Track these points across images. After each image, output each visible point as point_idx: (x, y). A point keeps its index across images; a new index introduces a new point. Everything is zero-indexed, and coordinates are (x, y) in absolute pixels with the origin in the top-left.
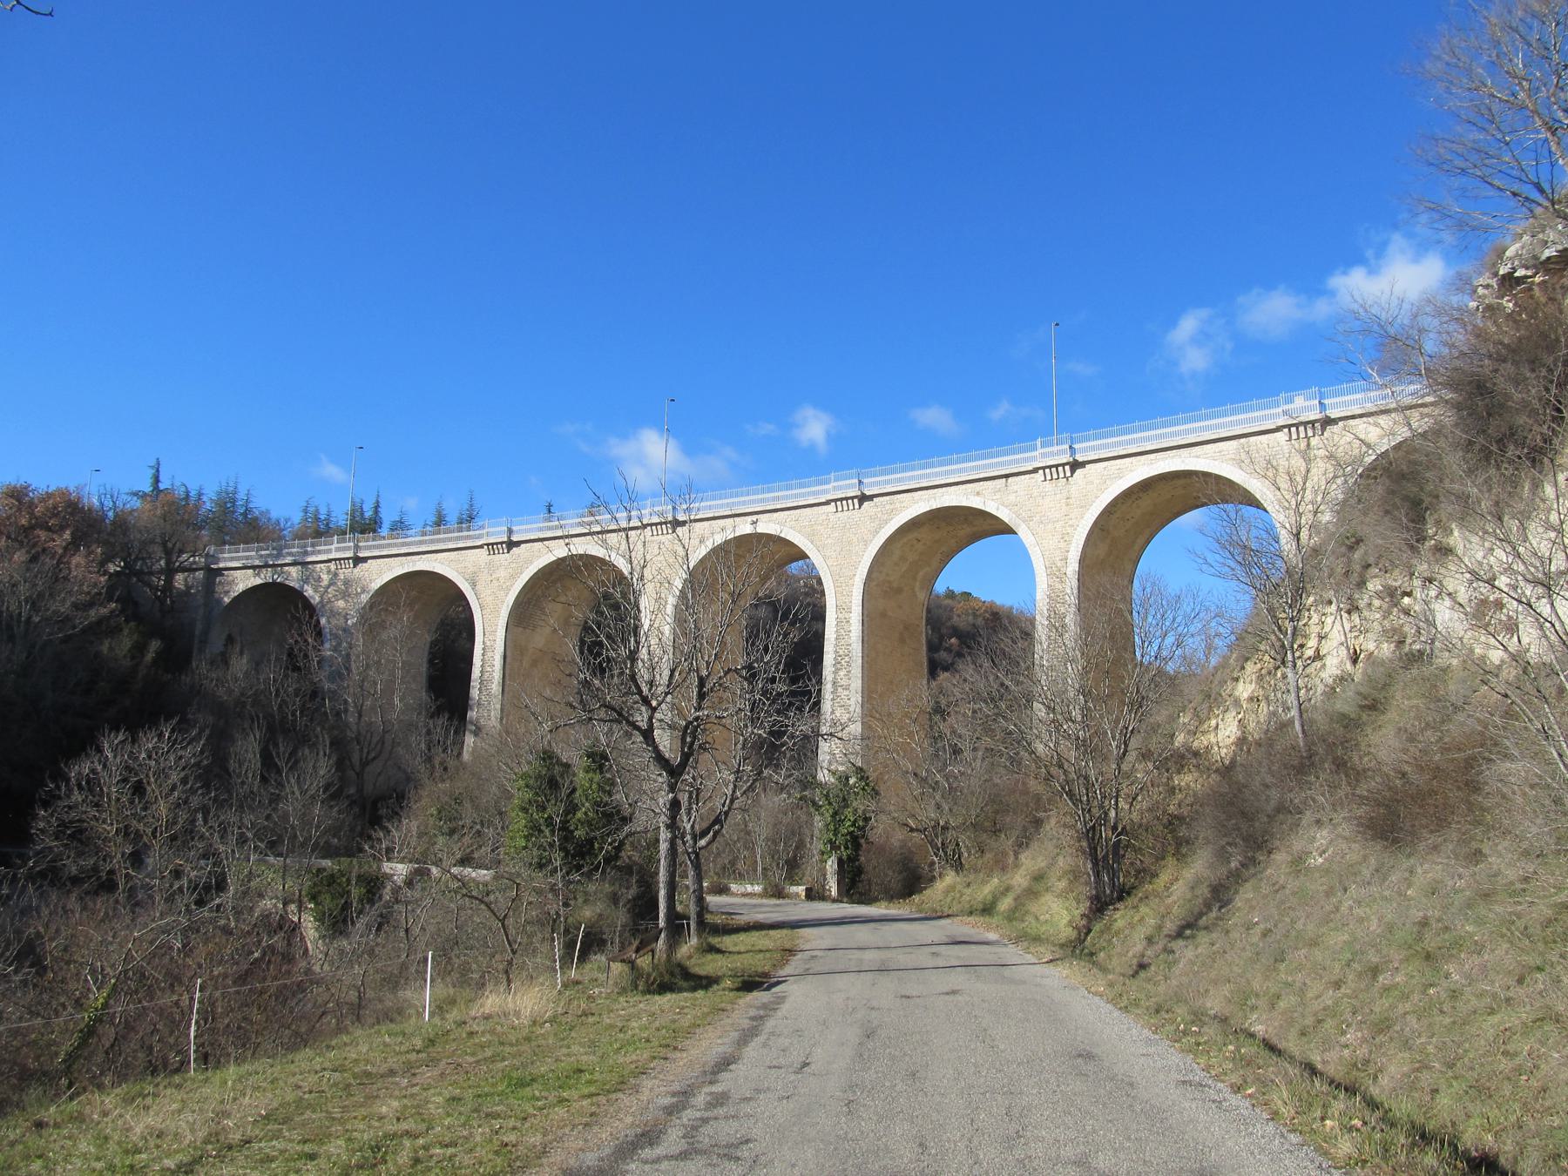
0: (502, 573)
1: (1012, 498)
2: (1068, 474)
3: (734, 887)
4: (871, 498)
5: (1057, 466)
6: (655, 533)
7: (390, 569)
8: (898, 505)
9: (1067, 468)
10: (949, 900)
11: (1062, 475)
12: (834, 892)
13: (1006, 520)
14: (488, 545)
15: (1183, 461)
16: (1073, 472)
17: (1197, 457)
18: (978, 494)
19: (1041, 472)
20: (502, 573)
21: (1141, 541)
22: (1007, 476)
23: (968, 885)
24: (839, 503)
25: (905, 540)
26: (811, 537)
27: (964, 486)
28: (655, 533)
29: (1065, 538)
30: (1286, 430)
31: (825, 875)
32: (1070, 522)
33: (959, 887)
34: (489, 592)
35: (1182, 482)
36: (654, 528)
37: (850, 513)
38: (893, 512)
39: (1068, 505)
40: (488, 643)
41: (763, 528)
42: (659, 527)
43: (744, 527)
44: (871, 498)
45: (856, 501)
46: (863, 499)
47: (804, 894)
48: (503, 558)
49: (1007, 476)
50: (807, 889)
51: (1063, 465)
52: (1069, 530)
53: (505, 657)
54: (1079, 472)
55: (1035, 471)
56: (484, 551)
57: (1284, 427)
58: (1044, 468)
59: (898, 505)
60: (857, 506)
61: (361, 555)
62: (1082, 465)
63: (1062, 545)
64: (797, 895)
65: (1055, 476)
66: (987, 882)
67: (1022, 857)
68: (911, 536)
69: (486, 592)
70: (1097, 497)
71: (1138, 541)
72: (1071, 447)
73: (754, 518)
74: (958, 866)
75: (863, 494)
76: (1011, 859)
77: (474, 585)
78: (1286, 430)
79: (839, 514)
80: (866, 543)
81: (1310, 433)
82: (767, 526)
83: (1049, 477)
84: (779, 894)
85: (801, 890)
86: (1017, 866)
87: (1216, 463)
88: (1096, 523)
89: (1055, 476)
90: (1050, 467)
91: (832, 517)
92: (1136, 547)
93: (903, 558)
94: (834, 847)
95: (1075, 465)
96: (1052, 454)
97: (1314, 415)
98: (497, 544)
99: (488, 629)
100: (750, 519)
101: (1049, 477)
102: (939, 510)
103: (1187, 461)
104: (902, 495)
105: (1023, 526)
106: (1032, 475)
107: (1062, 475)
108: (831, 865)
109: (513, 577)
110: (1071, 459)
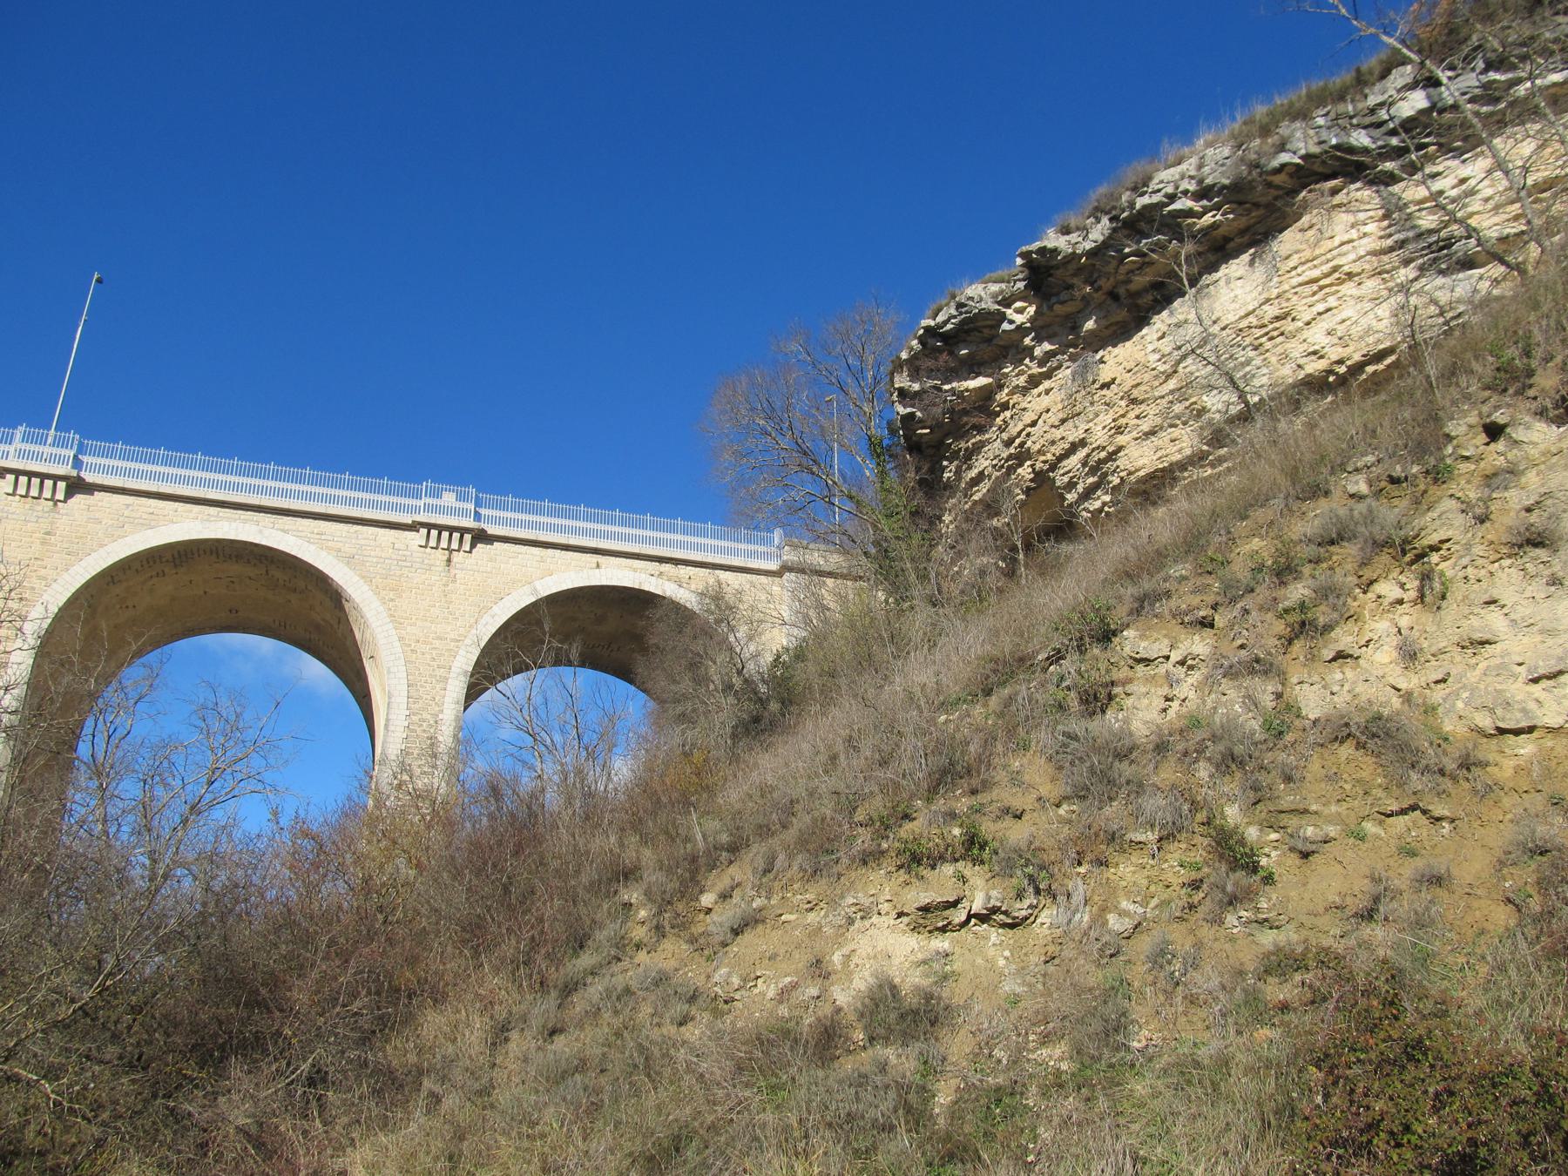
2: (60, 495)
5: (43, 477)
9: (62, 485)
11: (47, 494)
15: (261, 532)
16: (69, 494)
17: (283, 531)
19: (11, 478)
30: (424, 531)
32: (43, 572)
35: (235, 569)
51: (56, 478)
52: (37, 584)
54: (79, 499)
57: (423, 525)
58: (18, 473)
62: (90, 489)
65: (34, 492)
70: (102, 546)
72: (75, 457)
78: (424, 531)
81: (455, 545)
87: (312, 547)
88: (87, 586)
89: (34, 492)
90: (31, 475)
95: (77, 486)
96: (38, 457)
97: (469, 523)
101: (22, 490)
103: (267, 532)
107: (47, 494)
110: (74, 473)
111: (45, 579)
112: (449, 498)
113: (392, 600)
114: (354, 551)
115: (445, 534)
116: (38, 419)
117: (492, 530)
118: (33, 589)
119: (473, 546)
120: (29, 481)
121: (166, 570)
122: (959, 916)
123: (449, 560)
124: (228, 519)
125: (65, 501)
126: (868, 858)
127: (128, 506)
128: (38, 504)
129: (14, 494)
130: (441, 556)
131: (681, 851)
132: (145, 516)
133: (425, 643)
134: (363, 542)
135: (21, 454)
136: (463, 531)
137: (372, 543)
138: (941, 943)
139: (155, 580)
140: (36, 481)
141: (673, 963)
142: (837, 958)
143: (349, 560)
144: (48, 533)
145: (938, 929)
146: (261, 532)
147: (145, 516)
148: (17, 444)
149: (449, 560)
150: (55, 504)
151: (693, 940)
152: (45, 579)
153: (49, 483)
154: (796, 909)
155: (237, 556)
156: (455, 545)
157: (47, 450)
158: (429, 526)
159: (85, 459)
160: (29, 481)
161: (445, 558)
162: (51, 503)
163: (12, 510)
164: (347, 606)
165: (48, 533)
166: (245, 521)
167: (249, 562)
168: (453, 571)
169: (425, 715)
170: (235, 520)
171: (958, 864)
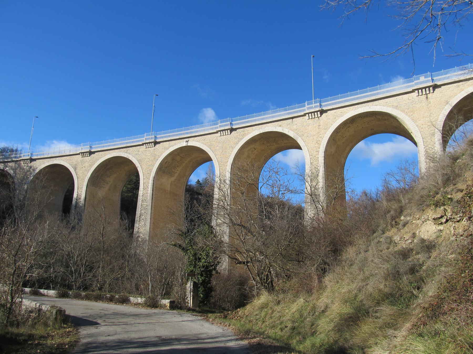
0: (87, 164)
1: (295, 127)
2: (319, 116)
3: (132, 299)
4: (236, 129)
5: (314, 112)
6: (147, 147)
7: (44, 163)
8: (246, 132)
9: (319, 113)
10: (263, 314)
11: (316, 116)
12: (190, 302)
13: (292, 136)
14: (82, 153)
15: (370, 108)
17: (376, 105)
18: (280, 126)
19: (307, 115)
20: (87, 164)
21: (348, 149)
22: (292, 118)
23: (279, 303)
24: (222, 132)
25: (249, 148)
26: (210, 147)
27: (274, 123)
28: (147, 147)
29: (318, 142)
30: (417, 91)
31: (185, 293)
32: (320, 136)
33: (271, 304)
34: (81, 172)
35: (367, 119)
36: (147, 145)
37: (226, 136)
38: (244, 135)
39: (319, 129)
40: (79, 192)
41: (190, 144)
42: (149, 144)
43: (183, 144)
44: (236, 129)
45: (229, 131)
46: (232, 130)
47: (168, 305)
48: (88, 159)
49: (292, 118)
50: (171, 302)
51: (317, 112)
53: (85, 198)
55: (305, 115)
56: (80, 156)
57: (416, 90)
59: (246, 132)
60: (229, 133)
61: (33, 158)
62: (326, 111)
63: (317, 145)
64: (165, 306)
65: (313, 117)
66: (294, 301)
67: (327, 279)
68: (252, 146)
69: (80, 172)
70: (332, 125)
71: (347, 148)
73: (187, 140)
74: (270, 288)
75: (232, 128)
76: (316, 283)
77: (75, 169)
78: (417, 91)
79: (222, 137)
80: (233, 148)
81: (428, 92)
82: (193, 143)
83: (311, 117)
84: (153, 304)
85: (166, 302)
86: (322, 288)
87: (385, 107)
88: (331, 136)
89: (313, 117)
90: (311, 113)
91: (219, 138)
92: (346, 152)
93: (248, 156)
94: (192, 274)
95: (322, 112)
96: (312, 108)
97: (430, 84)
98: (85, 152)
99: (80, 186)
100: (185, 140)
101: (311, 117)
102: (263, 133)
103: (372, 107)
104: (248, 128)
105: (300, 138)
106: (303, 117)
107: (316, 116)
108: (189, 286)
109: (91, 166)
110: (321, 109)
111: (321, 137)
112: (422, 78)
113: (412, 115)
114: (397, 104)
115: (424, 90)
116: (309, 99)
117: (439, 83)
118: (319, 140)
119: (434, 90)
120: (311, 114)
121: (350, 125)
122: (444, 220)
123: (427, 97)
124: (360, 107)
125: (321, 116)
126: (429, 206)
127: (335, 112)
128: (315, 119)
129: (309, 119)
130: (424, 97)
131: (400, 205)
132: (340, 114)
133: (425, 125)
134: (399, 101)
135: (308, 108)
136: (429, 87)
137: (402, 100)
138: (441, 227)
139: (348, 129)
140: (313, 114)
141: (393, 234)
142: (417, 232)
143: (396, 107)
144: (319, 126)
145: (440, 224)
146: (370, 108)
147: (340, 114)
148: (307, 106)
149: (427, 97)
150: (319, 118)
151: (398, 228)
152: (321, 137)
153: (316, 113)
154: (416, 219)
155: (366, 116)
156: (428, 92)
157: (313, 105)
158: (418, 89)
159: (323, 104)
160: (311, 114)
161: (426, 97)
162: (318, 118)
163: (310, 123)
164: (399, 120)
165: (319, 126)
166: (365, 106)
167: (370, 116)
168: (429, 100)
169: (430, 146)
170: (362, 107)
171: (445, 206)
